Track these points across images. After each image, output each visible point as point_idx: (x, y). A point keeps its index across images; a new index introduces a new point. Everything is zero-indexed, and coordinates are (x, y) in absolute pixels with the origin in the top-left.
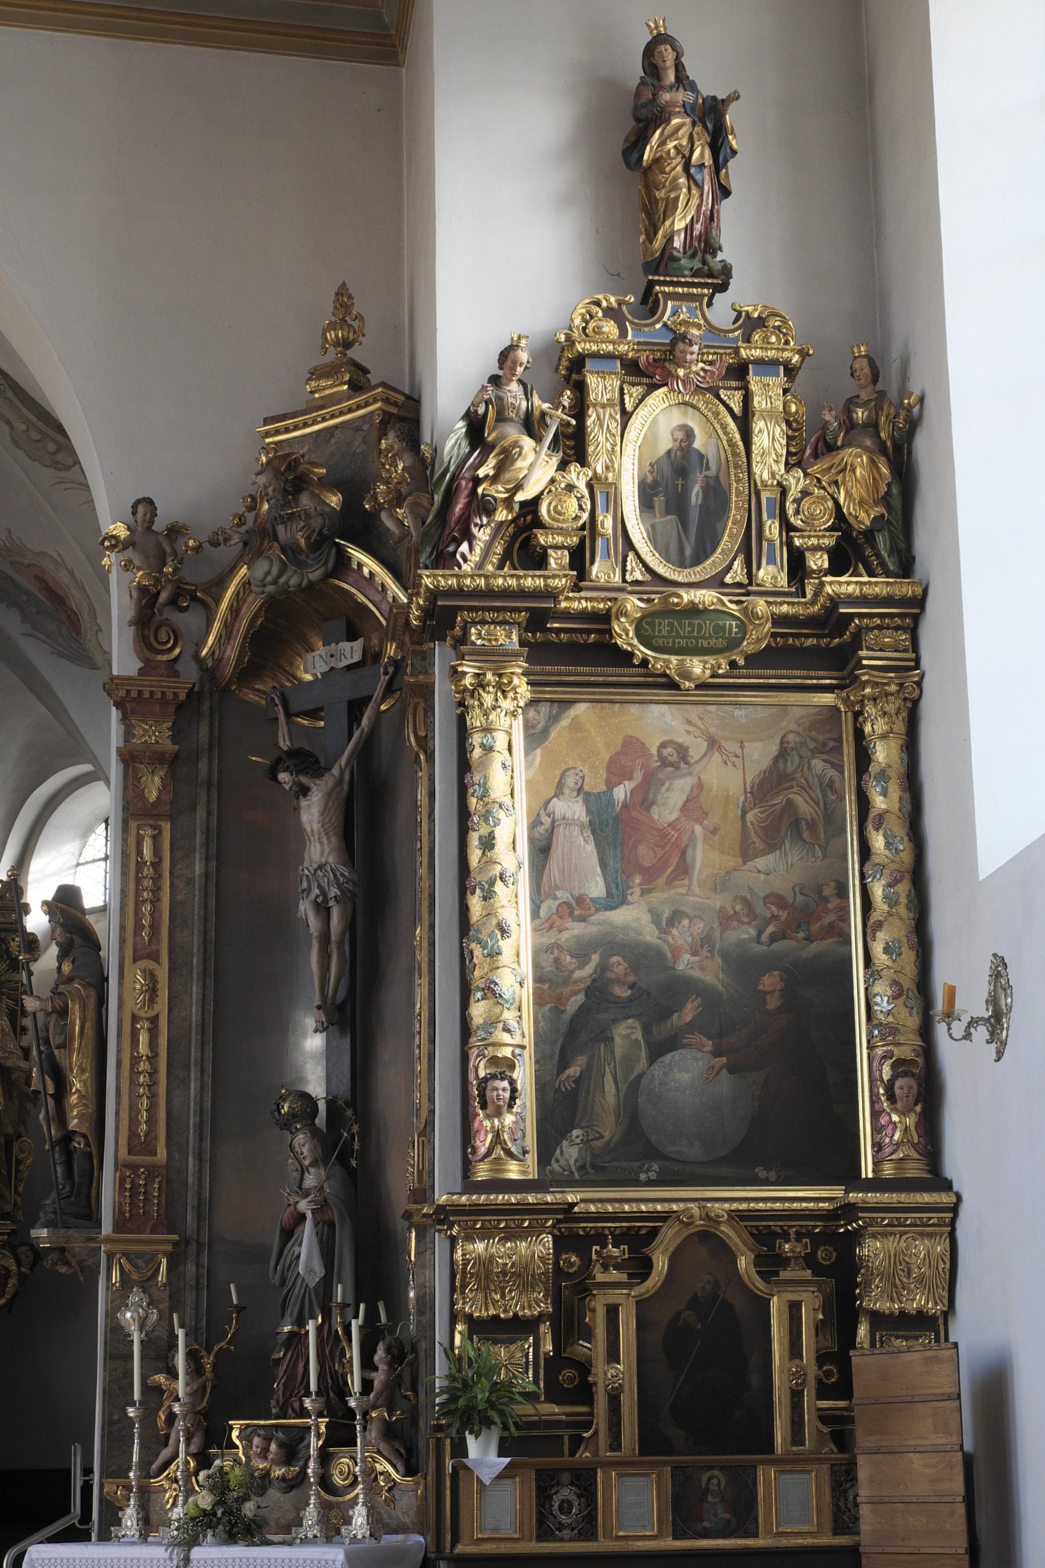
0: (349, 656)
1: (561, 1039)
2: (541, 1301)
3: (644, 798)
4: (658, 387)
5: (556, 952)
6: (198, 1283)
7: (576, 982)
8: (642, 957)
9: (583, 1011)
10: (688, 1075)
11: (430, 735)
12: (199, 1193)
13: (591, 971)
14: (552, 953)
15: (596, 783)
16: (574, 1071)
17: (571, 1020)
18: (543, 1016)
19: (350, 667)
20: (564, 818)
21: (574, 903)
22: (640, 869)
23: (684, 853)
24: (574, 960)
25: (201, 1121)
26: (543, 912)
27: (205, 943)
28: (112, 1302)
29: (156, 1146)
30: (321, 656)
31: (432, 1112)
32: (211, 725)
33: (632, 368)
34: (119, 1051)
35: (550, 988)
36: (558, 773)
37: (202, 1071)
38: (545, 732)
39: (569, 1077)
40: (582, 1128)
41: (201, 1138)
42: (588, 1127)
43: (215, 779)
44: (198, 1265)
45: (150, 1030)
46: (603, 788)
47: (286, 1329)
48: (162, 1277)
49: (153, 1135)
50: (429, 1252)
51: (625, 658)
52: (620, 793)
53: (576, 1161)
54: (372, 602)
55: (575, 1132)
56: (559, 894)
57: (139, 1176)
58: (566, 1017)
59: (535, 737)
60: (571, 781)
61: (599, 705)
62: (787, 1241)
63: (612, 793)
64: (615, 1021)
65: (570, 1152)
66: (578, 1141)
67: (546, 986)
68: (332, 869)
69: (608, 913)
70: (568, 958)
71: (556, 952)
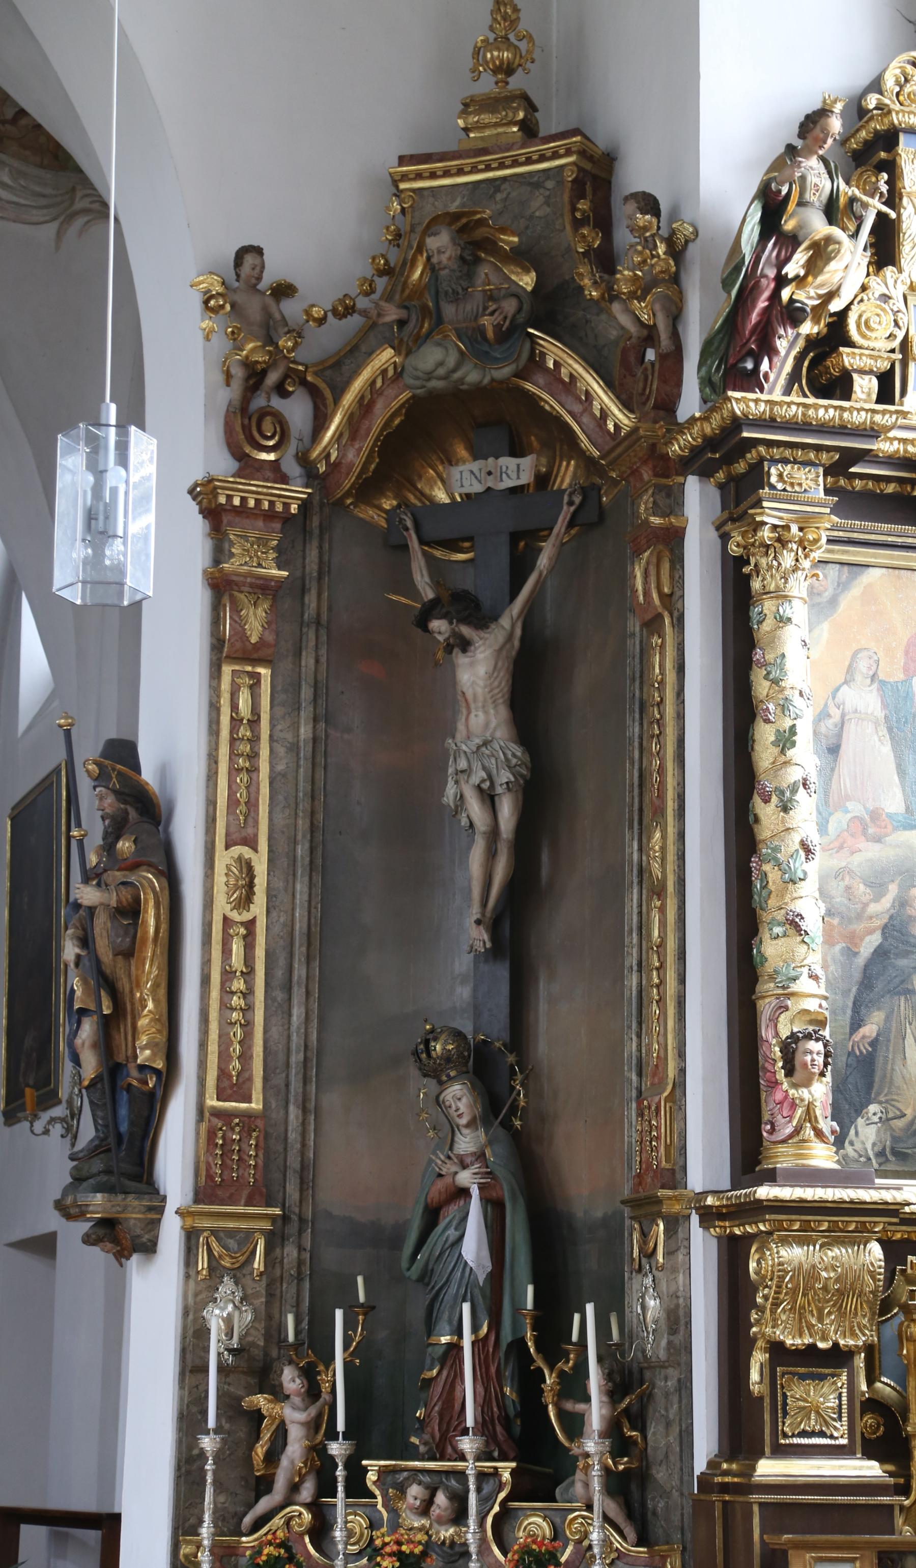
0: (514, 476)
1: (854, 989)
2: (865, 1326)
5: (847, 878)
6: (299, 1272)
7: (871, 918)
9: (880, 953)
11: (678, 593)
12: (303, 1153)
13: (888, 905)
14: (843, 879)
15: (893, 672)
16: (869, 1030)
17: (866, 967)
18: (834, 959)
19: (513, 490)
20: (856, 711)
21: (867, 817)
24: (868, 891)
25: (306, 1058)
26: (832, 827)
27: (313, 828)
28: (196, 1295)
29: (250, 1090)
30: (472, 472)
31: (682, 1071)
32: (320, 547)
34: (206, 963)
35: (840, 924)
36: (849, 654)
37: (308, 993)
38: (833, 602)
39: (864, 1037)
40: (880, 1103)
41: (306, 1081)
42: (887, 1102)
43: (324, 617)
44: (301, 1249)
45: (245, 937)
46: (901, 676)
47: (444, 1340)
48: (258, 1263)
49: (246, 1075)
50: (683, 1251)
53: (874, 1144)
54: (570, 413)
55: (873, 1108)
56: (850, 805)
57: (233, 1129)
58: (861, 961)
59: (822, 607)
60: (863, 665)
61: (897, 571)
63: (911, 684)
65: (867, 1134)
66: (876, 1119)
67: (836, 921)
68: (501, 747)
69: (907, 833)
70: (862, 886)
71: (847, 878)
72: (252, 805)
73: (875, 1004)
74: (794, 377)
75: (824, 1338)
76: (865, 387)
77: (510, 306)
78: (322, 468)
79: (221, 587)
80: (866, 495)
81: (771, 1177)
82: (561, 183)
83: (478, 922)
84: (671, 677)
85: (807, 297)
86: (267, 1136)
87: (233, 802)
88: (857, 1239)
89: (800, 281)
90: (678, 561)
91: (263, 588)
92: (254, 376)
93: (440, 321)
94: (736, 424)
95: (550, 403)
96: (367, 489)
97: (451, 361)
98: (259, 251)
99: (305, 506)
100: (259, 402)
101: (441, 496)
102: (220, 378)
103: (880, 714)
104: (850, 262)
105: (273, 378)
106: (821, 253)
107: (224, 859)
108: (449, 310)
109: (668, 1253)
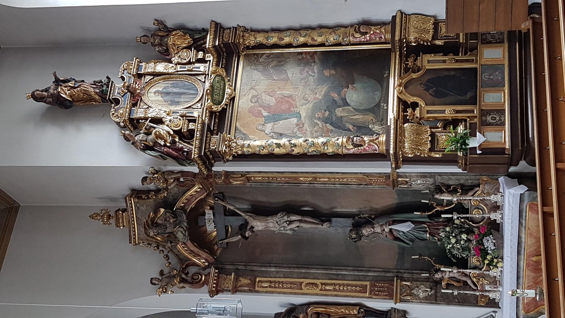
3: (267, 108)
4: (141, 99)
8: (316, 108)
10: (355, 95)
16: (351, 127)
19: (214, 215)
22: (289, 109)
23: (285, 96)
27: (298, 268)
31: (361, 173)
33: (134, 105)
34: (332, 295)
37: (340, 269)
38: (244, 134)
41: (362, 271)
44: (405, 273)
47: (428, 236)
51: (224, 111)
52: (265, 114)
55: (370, 127)
58: (334, 129)
59: (246, 138)
60: (260, 128)
62: (408, 64)
64: (336, 115)
65: (376, 128)
72: (291, 283)
73: (344, 126)
74: (189, 143)
75: (428, 138)
76: (192, 126)
77: (168, 214)
78: (207, 264)
79: (235, 290)
80: (218, 127)
81: (388, 150)
82: (138, 202)
83: (322, 225)
84: (262, 175)
85: (169, 139)
86: (376, 281)
87: (291, 288)
88: (403, 130)
89: (165, 141)
90: (233, 173)
91: (236, 279)
92: (183, 281)
93: (171, 233)
94: (200, 156)
95: (193, 205)
96: (212, 252)
97: (181, 230)
98: (152, 279)
99: (216, 268)
100: (189, 279)
101: (215, 233)
102: (183, 289)
103: (272, 124)
104: (162, 129)
105: (184, 276)
106: (159, 136)
107: (305, 290)
108: (168, 230)
109: (407, 177)
